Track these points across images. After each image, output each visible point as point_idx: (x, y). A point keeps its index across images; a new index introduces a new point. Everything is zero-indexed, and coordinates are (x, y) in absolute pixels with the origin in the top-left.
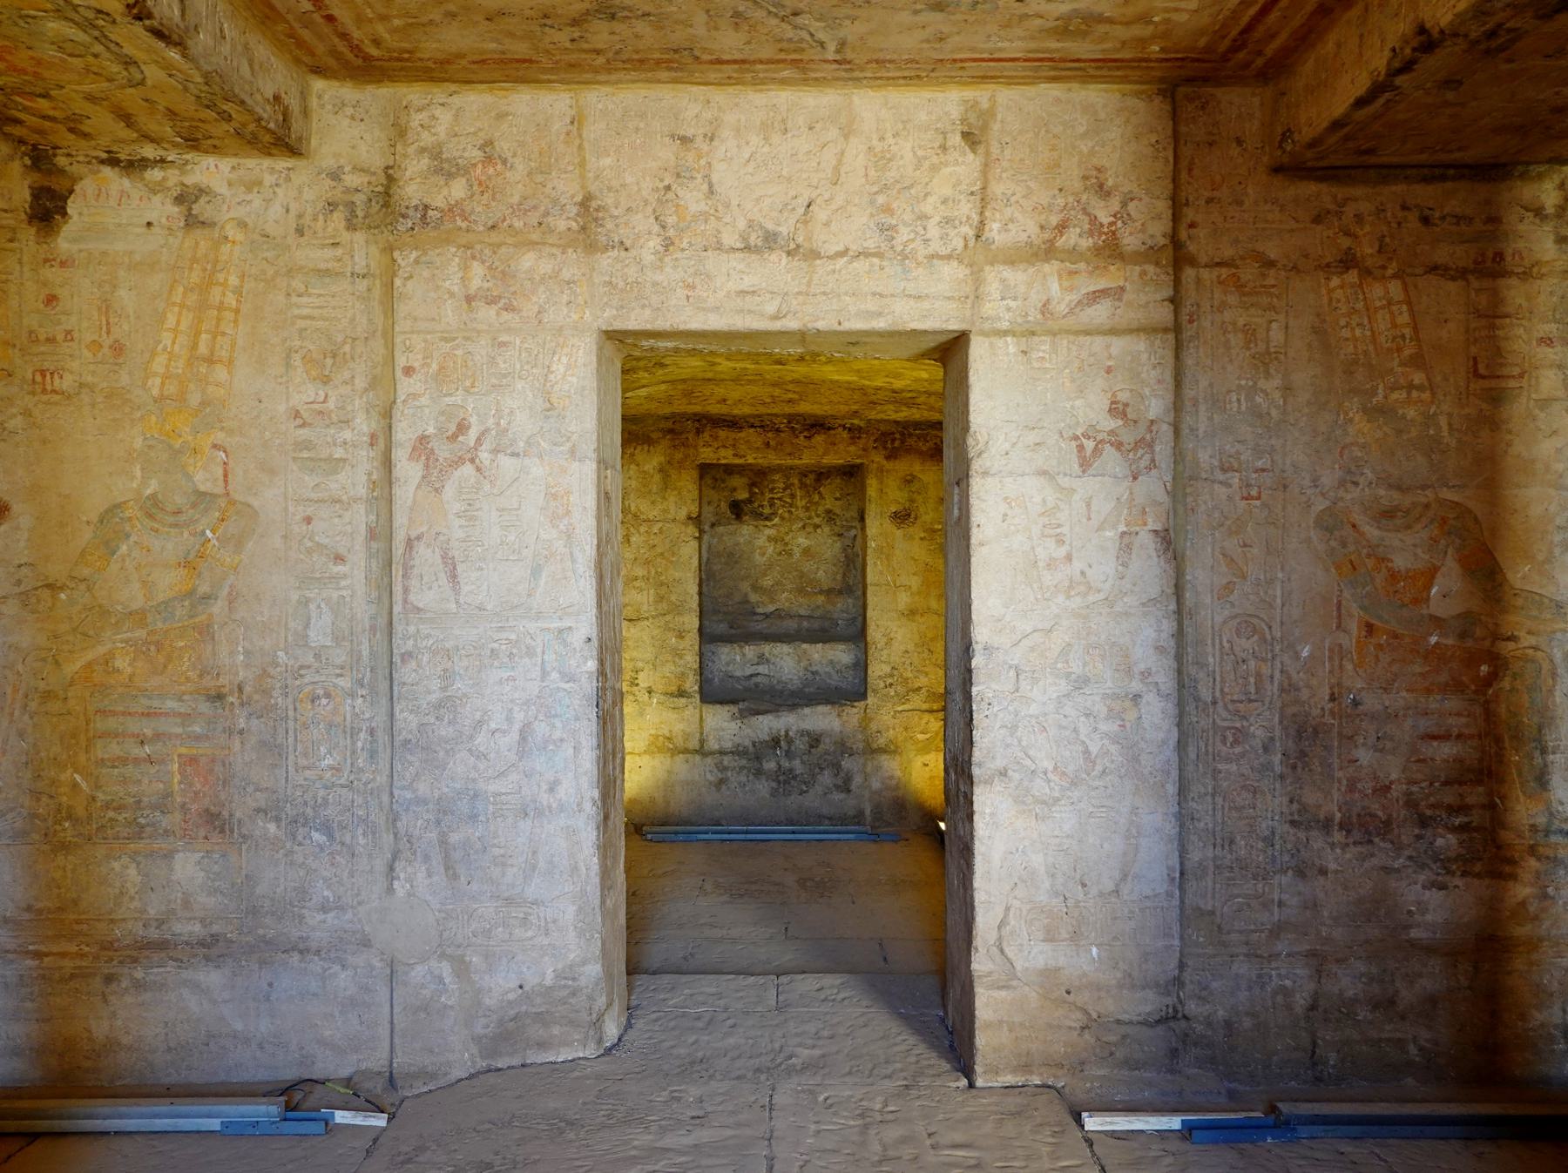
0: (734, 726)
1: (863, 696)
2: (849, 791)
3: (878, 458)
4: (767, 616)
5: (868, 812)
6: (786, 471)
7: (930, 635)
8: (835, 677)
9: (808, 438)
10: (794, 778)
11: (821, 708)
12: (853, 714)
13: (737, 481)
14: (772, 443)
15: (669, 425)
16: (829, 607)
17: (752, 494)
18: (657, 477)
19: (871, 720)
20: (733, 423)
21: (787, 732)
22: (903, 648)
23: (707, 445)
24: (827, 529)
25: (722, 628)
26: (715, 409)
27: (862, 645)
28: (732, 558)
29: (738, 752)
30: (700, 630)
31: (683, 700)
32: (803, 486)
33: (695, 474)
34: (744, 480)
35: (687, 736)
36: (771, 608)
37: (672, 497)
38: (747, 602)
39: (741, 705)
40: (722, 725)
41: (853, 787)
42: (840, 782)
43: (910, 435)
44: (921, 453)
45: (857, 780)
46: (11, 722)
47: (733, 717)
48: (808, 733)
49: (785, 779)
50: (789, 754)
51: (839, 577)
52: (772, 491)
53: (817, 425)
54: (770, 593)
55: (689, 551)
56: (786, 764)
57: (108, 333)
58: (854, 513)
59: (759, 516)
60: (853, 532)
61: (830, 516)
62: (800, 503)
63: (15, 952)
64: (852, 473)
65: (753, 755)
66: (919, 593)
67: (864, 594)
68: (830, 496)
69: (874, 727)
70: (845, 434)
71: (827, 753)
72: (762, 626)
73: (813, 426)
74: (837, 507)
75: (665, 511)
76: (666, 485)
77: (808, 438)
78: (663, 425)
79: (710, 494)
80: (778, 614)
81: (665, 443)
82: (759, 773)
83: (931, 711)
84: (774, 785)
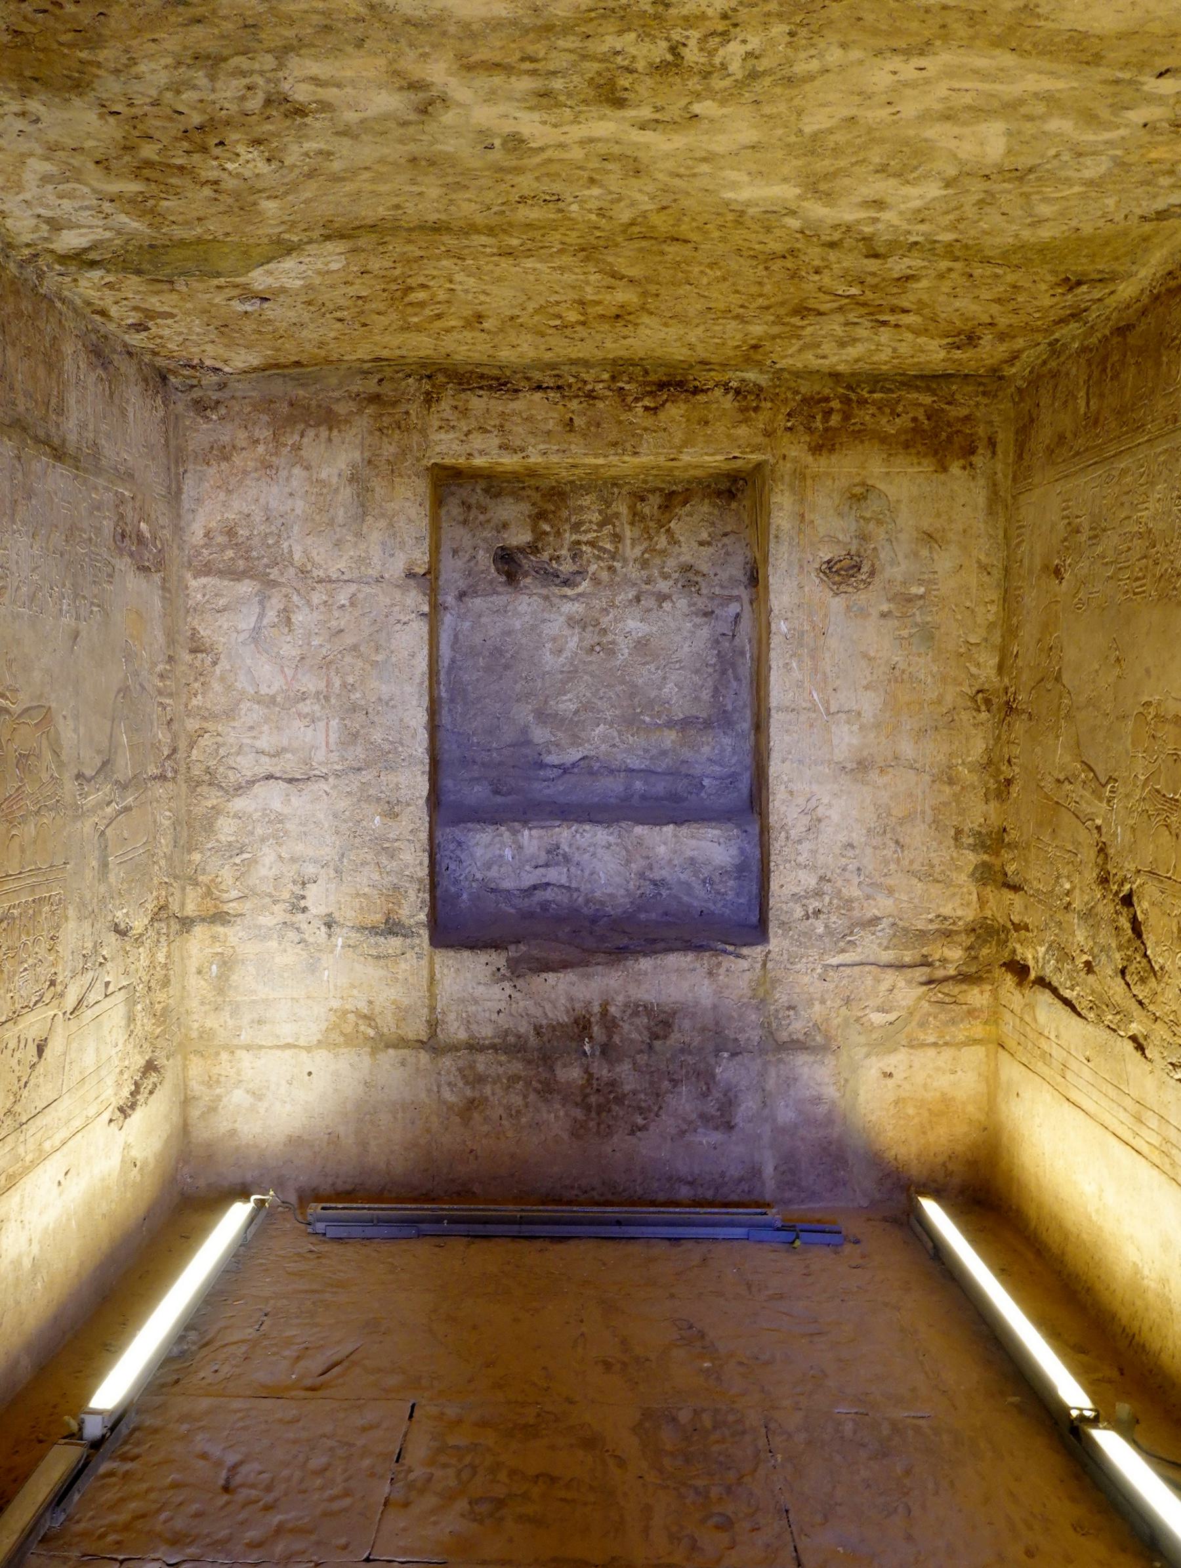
0: (495, 995)
2: (730, 1127)
3: (796, 450)
4: (565, 770)
5: (769, 1170)
6: (605, 487)
7: (898, 812)
9: (655, 410)
10: (619, 1100)
13: (509, 510)
14: (579, 422)
15: (371, 386)
16: (686, 753)
18: (347, 493)
19: (775, 982)
20: (499, 382)
21: (605, 1006)
22: (842, 838)
23: (446, 426)
24: (682, 603)
25: (478, 793)
26: (466, 348)
27: (755, 829)
28: (500, 659)
29: (508, 1045)
30: (435, 800)
31: (395, 942)
33: (422, 486)
34: (525, 508)
35: (403, 1013)
36: (573, 755)
37: (376, 534)
38: (528, 743)
39: (513, 952)
40: (472, 988)
41: (738, 1120)
42: (711, 1107)
43: (862, 402)
44: (884, 439)
45: (748, 1105)
48: (648, 1009)
49: (599, 1105)
50: (606, 1050)
51: (706, 695)
53: (671, 384)
54: (572, 726)
55: (410, 641)
56: (602, 1071)
59: (549, 576)
60: (734, 608)
61: (689, 577)
62: (632, 551)
65: (538, 1052)
66: (877, 726)
67: (760, 726)
69: (781, 997)
71: (685, 1049)
72: (557, 790)
73: (662, 386)
74: (703, 559)
76: (363, 507)
77: (653, 410)
78: (357, 386)
79: (454, 534)
80: (587, 767)
81: (363, 423)
82: (548, 1089)
83: (900, 967)
84: (579, 1113)
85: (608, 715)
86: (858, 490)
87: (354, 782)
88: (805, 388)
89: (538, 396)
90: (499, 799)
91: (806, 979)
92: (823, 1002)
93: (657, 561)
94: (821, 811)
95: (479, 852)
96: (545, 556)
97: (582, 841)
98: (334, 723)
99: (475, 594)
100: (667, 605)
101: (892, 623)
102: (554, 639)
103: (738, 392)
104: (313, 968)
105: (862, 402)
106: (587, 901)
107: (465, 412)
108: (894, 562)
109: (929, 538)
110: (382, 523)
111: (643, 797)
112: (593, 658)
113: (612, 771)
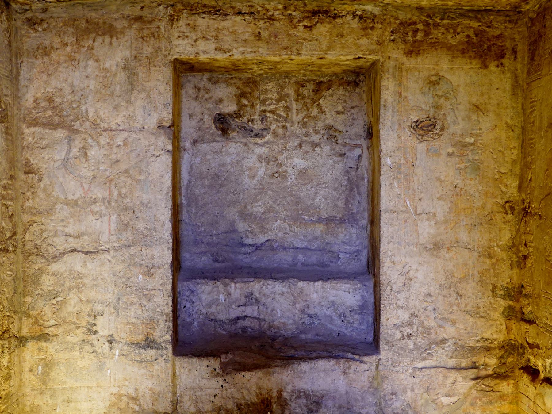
1: (373, 345)
3: (396, 53)
4: (257, 247)
7: (458, 275)
8: (338, 322)
9: (309, 28)
11: (322, 364)
12: (362, 371)
13: (223, 91)
16: (329, 238)
17: (242, 107)
18: (121, 76)
19: (384, 378)
21: (280, 392)
22: (424, 290)
24: (327, 148)
28: (217, 180)
31: (152, 353)
32: (299, 97)
33: (168, 72)
35: (156, 396)
36: (262, 239)
38: (235, 231)
39: (224, 358)
43: (436, 25)
44: (449, 48)
47: (214, 374)
51: (341, 203)
52: (263, 102)
54: (261, 222)
58: (359, 129)
61: (331, 133)
62: (297, 117)
64: (361, 79)
66: (446, 222)
68: (332, 108)
69: (387, 387)
70: (355, 24)
73: (315, 13)
75: (131, 118)
77: (309, 28)
80: (270, 246)
81: (132, 33)
83: (459, 369)
85: (283, 215)
86: (434, 78)
87: (126, 254)
88: (402, 16)
89: (239, 18)
90: (217, 265)
91: (403, 376)
92: (413, 390)
93: (312, 123)
94: (411, 274)
95: (204, 297)
96: (245, 119)
97: (266, 290)
98: (114, 217)
99: (203, 141)
100: (318, 150)
101: (455, 160)
102: (250, 169)
103: (361, 17)
104: (101, 368)
105: (436, 25)
106: (270, 327)
107: (194, 28)
108: (455, 123)
109: (477, 108)
110: (143, 95)
111: (303, 264)
112: (273, 181)
113: (285, 249)
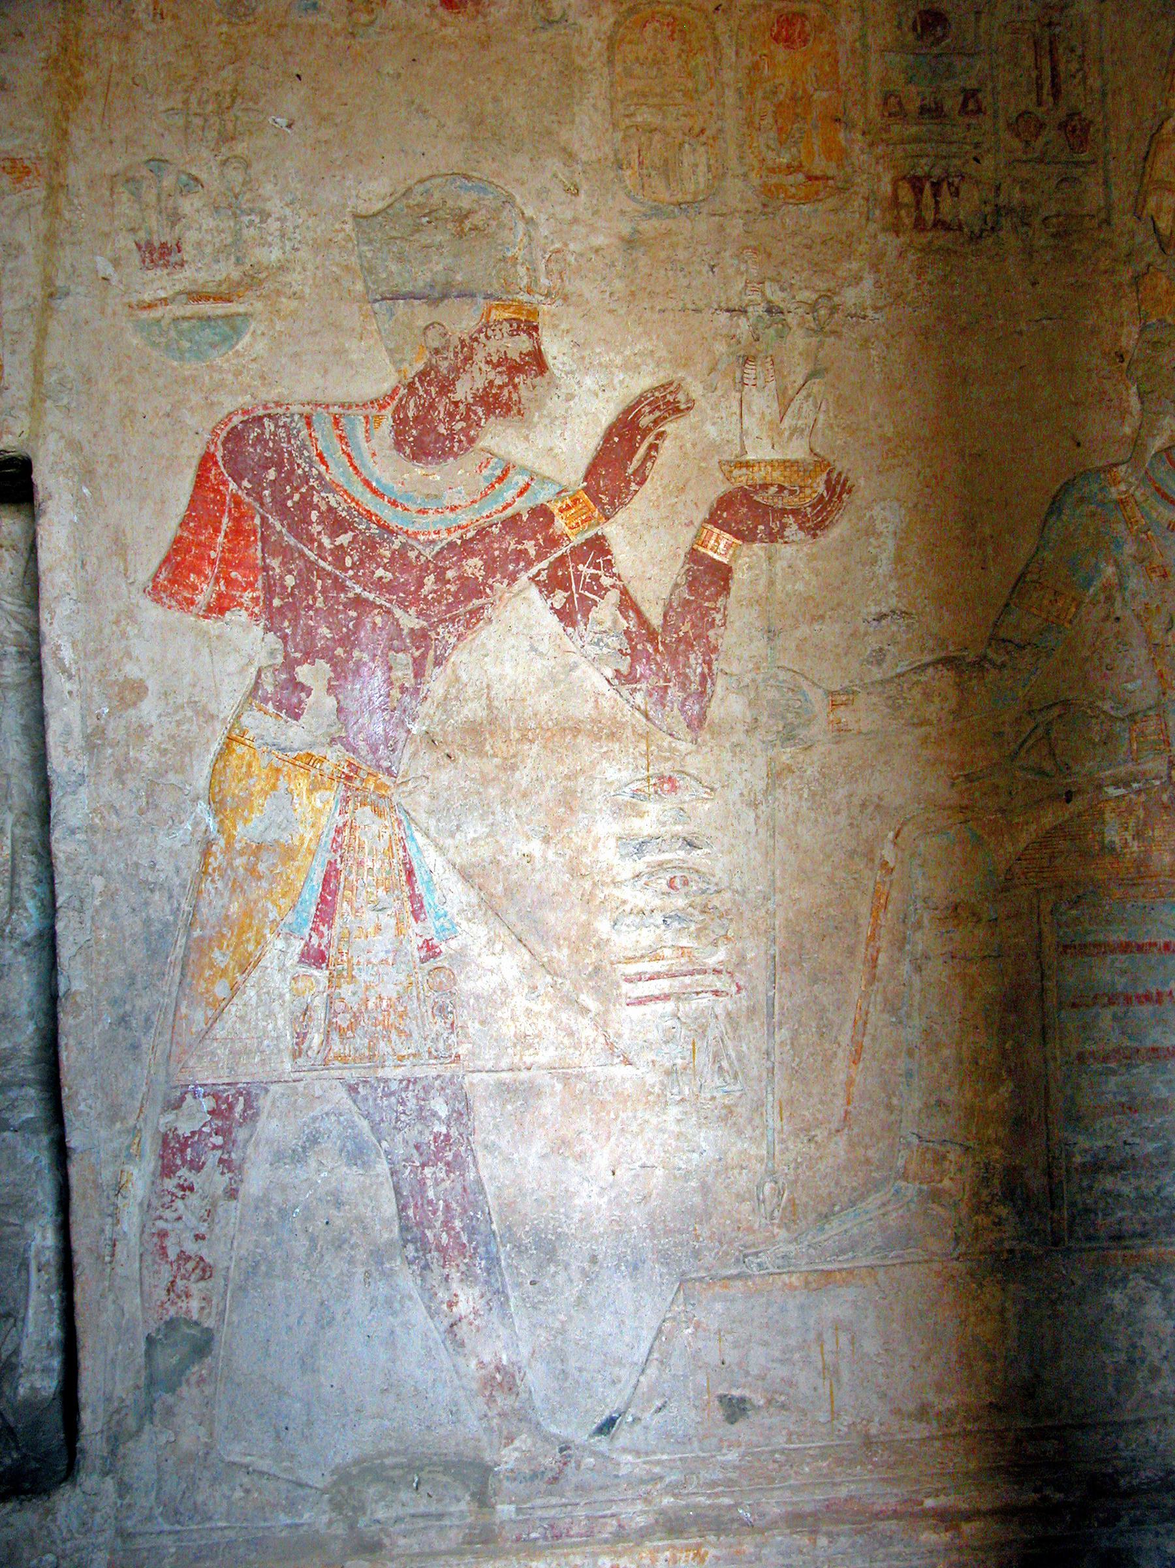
46: (873, 979)
57: (1056, 93)
63: (896, 1515)
